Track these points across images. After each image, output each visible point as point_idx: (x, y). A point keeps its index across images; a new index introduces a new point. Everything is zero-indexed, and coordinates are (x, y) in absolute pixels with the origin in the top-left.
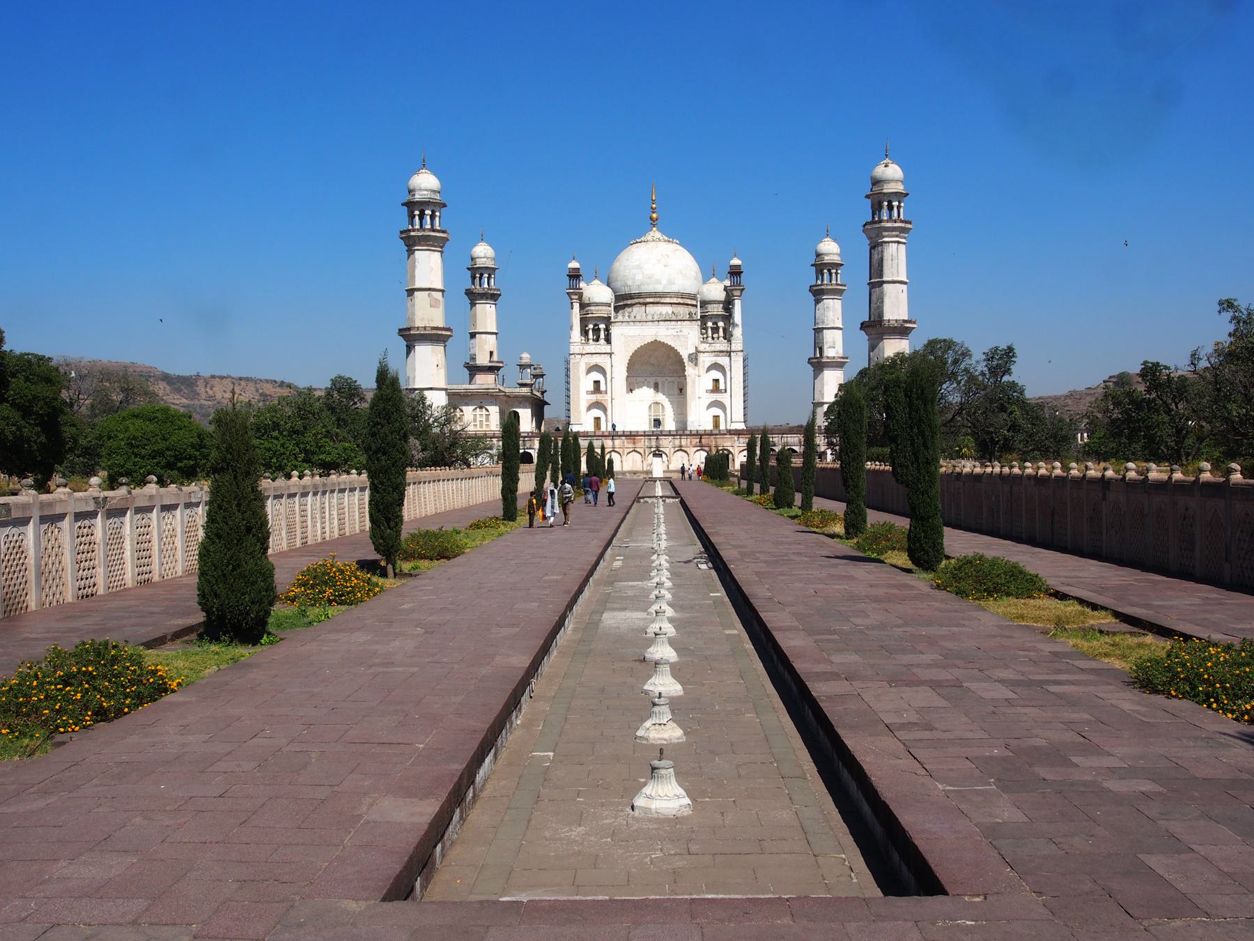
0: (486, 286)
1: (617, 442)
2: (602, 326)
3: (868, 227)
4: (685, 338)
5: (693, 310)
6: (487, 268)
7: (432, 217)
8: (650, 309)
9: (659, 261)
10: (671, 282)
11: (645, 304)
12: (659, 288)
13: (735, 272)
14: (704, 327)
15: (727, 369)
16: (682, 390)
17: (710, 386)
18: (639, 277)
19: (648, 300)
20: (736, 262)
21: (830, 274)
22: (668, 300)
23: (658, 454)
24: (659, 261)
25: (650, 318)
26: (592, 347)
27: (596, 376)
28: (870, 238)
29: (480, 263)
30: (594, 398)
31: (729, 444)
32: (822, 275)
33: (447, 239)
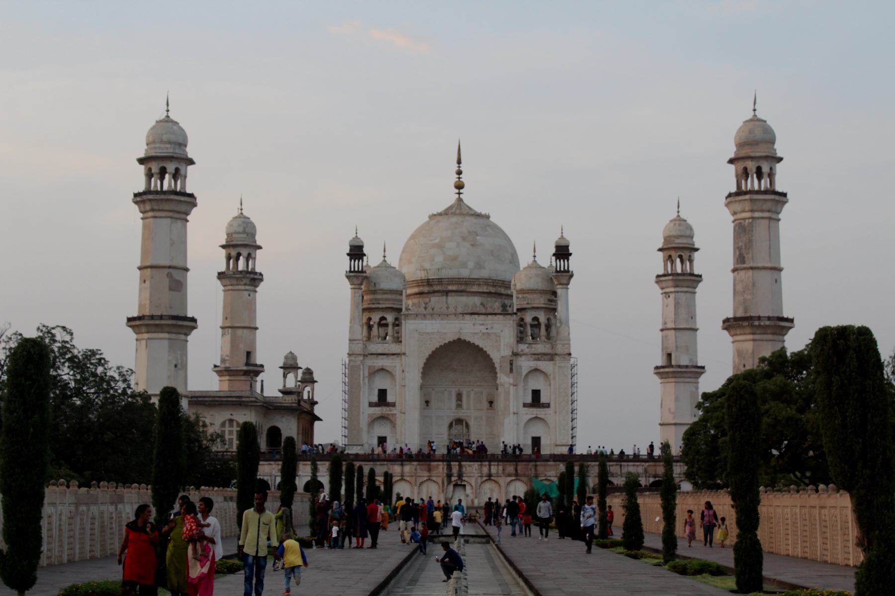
1: (407, 468)
2: (390, 318)
3: (729, 200)
4: (497, 336)
5: (507, 302)
6: (245, 246)
7: (176, 175)
8: (452, 300)
10: (479, 266)
11: (447, 293)
12: (465, 273)
14: (521, 324)
16: (491, 403)
17: (529, 400)
18: (439, 259)
19: (450, 288)
20: (563, 243)
21: (682, 262)
22: (475, 289)
23: (460, 485)
24: (464, 239)
25: (451, 310)
27: (382, 382)
28: (734, 213)
29: (240, 239)
30: (378, 411)
32: (673, 262)
33: (195, 205)
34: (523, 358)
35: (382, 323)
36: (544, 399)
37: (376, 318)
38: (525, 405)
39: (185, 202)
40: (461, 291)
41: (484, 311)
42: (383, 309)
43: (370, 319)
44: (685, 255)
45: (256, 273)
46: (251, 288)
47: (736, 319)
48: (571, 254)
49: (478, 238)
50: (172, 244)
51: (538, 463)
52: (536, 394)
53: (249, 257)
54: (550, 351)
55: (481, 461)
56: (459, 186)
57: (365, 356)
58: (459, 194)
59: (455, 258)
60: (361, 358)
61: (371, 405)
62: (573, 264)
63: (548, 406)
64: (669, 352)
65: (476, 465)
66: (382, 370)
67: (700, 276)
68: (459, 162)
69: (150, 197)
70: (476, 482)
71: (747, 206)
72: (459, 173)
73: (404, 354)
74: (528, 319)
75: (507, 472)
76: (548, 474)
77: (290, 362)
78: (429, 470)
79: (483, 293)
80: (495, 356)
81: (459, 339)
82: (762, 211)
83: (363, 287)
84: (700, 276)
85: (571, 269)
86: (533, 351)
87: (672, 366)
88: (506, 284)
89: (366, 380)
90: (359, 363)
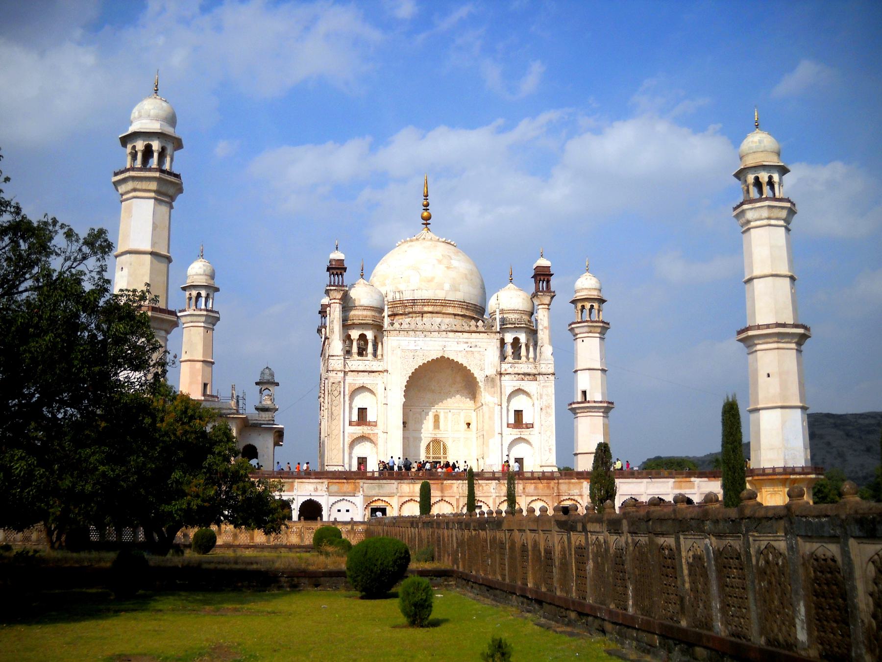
0: (203, 307)
9: (440, 262)
10: (454, 288)
11: (422, 313)
12: (441, 295)
13: (542, 276)
15: (535, 398)
16: (469, 424)
17: (512, 421)
19: (426, 309)
20: (543, 262)
22: (450, 310)
26: (356, 362)
27: (361, 401)
30: (359, 430)
31: (576, 491)
33: (182, 192)
34: (507, 376)
36: (526, 419)
37: (355, 334)
38: (508, 425)
39: (171, 182)
40: (437, 313)
41: (467, 328)
44: (596, 305)
46: (211, 326)
47: (759, 327)
49: (452, 261)
50: (155, 227)
51: (560, 481)
52: (518, 414)
54: (534, 371)
55: (498, 479)
57: (345, 373)
59: (431, 280)
60: (342, 374)
61: (351, 424)
63: (530, 426)
64: (584, 389)
65: (494, 482)
66: (363, 388)
67: (608, 324)
68: (427, 196)
69: (132, 174)
70: (494, 502)
71: (765, 213)
73: (387, 371)
74: (509, 338)
75: (527, 490)
76: (572, 492)
77: (267, 377)
78: (442, 491)
79: (458, 315)
80: (479, 376)
81: (442, 357)
82: (777, 219)
84: (608, 324)
85: (552, 289)
86: (516, 371)
87: (589, 402)
89: (347, 398)
90: (339, 380)
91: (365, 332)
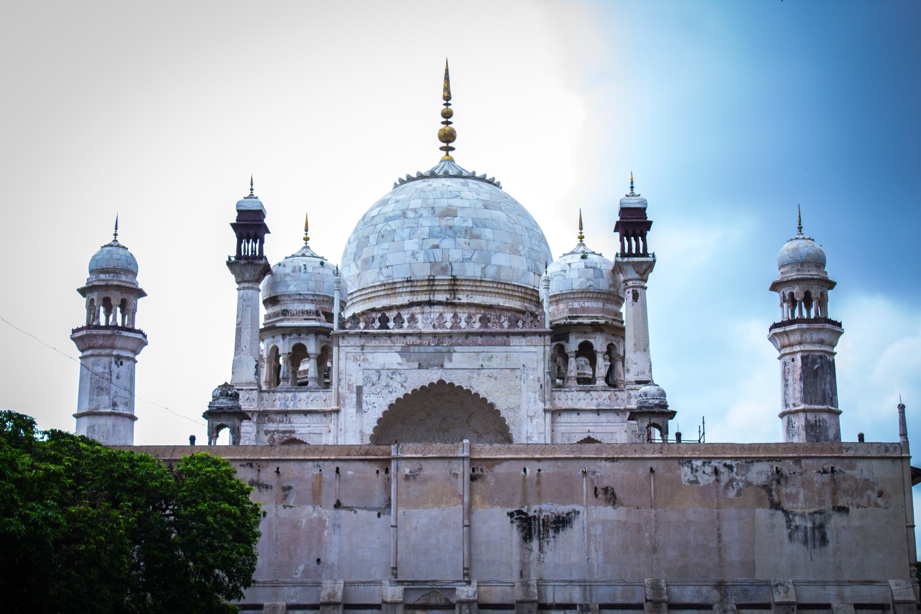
2: (312, 347)
14: (560, 356)
20: (633, 203)
35: (299, 353)
37: (285, 347)
42: (298, 330)
43: (275, 350)
45: (132, 330)
48: (651, 223)
53: (123, 305)
56: (448, 137)
58: (448, 149)
62: (655, 240)
68: (447, 98)
72: (447, 115)
74: (573, 345)
81: (441, 382)
83: (261, 286)
88: (532, 296)
91: (303, 342)
